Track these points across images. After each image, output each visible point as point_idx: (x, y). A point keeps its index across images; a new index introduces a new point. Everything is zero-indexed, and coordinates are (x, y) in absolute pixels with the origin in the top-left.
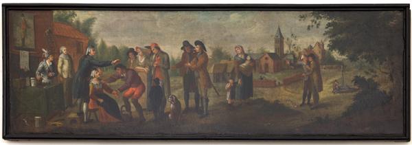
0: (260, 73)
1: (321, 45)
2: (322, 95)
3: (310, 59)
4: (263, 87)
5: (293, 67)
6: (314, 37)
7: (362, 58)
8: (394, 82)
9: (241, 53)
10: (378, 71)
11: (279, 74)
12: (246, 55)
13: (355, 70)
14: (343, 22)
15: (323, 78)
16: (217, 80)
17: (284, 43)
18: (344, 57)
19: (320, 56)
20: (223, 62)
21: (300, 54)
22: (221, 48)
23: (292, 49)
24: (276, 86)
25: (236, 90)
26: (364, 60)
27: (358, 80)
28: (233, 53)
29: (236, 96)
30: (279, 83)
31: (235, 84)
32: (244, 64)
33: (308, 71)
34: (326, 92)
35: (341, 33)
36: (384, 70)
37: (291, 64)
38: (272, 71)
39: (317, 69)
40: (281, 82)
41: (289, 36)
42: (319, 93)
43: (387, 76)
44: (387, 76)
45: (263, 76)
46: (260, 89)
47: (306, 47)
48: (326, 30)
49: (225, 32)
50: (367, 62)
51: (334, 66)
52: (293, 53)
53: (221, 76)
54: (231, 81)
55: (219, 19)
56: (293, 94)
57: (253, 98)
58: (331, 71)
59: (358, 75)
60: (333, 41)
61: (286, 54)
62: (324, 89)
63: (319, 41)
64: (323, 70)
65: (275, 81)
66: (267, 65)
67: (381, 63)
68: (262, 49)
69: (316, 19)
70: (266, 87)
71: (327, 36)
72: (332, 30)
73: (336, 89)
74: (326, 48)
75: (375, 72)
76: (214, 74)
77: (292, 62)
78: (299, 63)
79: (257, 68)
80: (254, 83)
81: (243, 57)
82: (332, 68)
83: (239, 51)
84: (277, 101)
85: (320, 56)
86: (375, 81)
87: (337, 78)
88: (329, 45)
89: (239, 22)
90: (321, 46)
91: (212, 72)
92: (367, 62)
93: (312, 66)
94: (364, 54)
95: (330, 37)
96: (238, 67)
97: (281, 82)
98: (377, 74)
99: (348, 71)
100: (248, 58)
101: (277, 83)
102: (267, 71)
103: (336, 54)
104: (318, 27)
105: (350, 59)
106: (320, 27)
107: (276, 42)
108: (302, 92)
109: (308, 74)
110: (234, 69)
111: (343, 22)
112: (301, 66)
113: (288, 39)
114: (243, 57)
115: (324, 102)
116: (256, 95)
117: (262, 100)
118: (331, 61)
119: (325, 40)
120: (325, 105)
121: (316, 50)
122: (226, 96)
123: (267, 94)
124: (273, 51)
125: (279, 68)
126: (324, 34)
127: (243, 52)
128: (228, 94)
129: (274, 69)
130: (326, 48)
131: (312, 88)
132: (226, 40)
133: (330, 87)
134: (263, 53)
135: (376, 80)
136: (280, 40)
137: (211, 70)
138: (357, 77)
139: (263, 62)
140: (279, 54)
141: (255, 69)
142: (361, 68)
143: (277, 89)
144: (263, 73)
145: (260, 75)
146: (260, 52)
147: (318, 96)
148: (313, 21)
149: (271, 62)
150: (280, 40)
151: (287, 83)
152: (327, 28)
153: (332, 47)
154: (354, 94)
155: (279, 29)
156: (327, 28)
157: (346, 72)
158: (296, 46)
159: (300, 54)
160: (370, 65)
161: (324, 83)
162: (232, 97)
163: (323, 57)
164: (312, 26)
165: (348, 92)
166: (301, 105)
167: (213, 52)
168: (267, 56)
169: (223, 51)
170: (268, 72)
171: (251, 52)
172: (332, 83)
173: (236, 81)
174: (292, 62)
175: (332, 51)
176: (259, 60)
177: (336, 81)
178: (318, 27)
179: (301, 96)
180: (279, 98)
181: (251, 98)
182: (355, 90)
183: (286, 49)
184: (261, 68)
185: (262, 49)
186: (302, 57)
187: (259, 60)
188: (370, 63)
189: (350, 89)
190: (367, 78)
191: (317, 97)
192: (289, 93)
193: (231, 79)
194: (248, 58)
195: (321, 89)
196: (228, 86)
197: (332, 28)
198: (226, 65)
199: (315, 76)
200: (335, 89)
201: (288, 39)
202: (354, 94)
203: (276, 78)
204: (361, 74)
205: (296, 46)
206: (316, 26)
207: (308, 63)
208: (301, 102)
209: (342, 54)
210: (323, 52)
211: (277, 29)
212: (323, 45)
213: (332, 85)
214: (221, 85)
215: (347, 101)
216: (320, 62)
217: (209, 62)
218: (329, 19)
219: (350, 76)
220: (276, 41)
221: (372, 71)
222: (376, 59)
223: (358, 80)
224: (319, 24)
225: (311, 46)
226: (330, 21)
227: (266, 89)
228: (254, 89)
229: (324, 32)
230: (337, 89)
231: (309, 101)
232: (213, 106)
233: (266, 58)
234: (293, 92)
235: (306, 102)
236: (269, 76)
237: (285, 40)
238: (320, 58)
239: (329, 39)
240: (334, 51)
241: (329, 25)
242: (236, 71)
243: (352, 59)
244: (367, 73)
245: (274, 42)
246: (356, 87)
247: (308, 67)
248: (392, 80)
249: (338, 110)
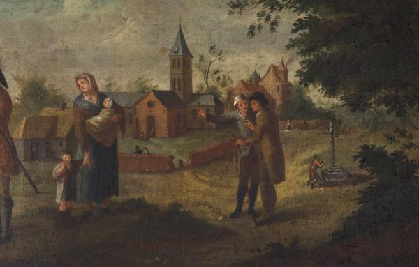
0: (137, 136)
1: (279, 72)
2: (283, 191)
3: (255, 106)
4: (142, 172)
6: (263, 53)
7: (378, 103)
9: (90, 92)
11: (181, 141)
12: (102, 97)
13: (360, 132)
14: (332, 17)
15: (287, 150)
16: (33, 156)
18: (336, 101)
19: (278, 98)
20: (47, 112)
21: (231, 94)
22: (44, 80)
24: (172, 169)
25: (79, 176)
26: (383, 108)
27: (368, 156)
28: (70, 92)
29: (78, 195)
30: (181, 161)
31: (75, 164)
32: (99, 118)
33: (251, 133)
34: (293, 184)
35: (328, 43)
37: (209, 117)
38: (165, 134)
39: (271, 130)
40: (186, 161)
41: (205, 51)
45: (142, 145)
46: (136, 176)
47: (245, 76)
48: (294, 36)
49: (52, 40)
50: (389, 112)
51: (312, 122)
52: (213, 92)
53: (42, 147)
54: (65, 157)
55: (37, 11)
57: (120, 198)
58: (305, 133)
60: (309, 63)
61: (199, 95)
62: (288, 175)
64: (284, 132)
65: (172, 157)
66: (151, 121)
69: (268, 10)
70: (150, 172)
71: (296, 49)
73: (316, 175)
74: (292, 78)
75: (411, 136)
76: (26, 141)
77: (212, 112)
78: (228, 114)
79: (127, 126)
81: (94, 101)
82: (306, 127)
83: (86, 86)
84: (176, 205)
85: (278, 98)
86: (410, 158)
87: (317, 151)
88: (299, 73)
89: (85, 17)
90: (281, 76)
91: (20, 135)
92: (389, 112)
93: (260, 122)
94: (383, 93)
95: (303, 53)
96: (83, 124)
98: (414, 141)
99: (345, 133)
100: (108, 103)
101: (176, 162)
102: (151, 134)
103: (316, 95)
104: (273, 29)
106: (280, 29)
108: (236, 183)
109: (250, 140)
110: (72, 132)
111: (332, 17)
112: (233, 122)
113: (202, 58)
114: (94, 101)
115: (289, 207)
116: (126, 192)
117: (140, 204)
118: (305, 110)
119: (291, 61)
120: (291, 216)
121: (270, 85)
122: (54, 193)
123: (150, 189)
124: (165, 86)
125: (179, 127)
126: (288, 47)
127: (94, 88)
128: (60, 190)
129: (169, 128)
130: (292, 78)
131: (259, 173)
132: (54, 60)
133: (303, 173)
134: (144, 91)
135: (411, 155)
136: (182, 61)
137: (18, 132)
138: (366, 147)
139: (143, 112)
140: (180, 94)
141: (123, 132)
142: (376, 126)
146: (135, 88)
148: (260, 15)
149: (161, 113)
150: (182, 61)
151: (200, 162)
152: (294, 31)
153: (308, 77)
154: (360, 187)
155: (181, 32)
156: (294, 31)
157: (341, 136)
158: (221, 75)
159: (231, 94)
160: (398, 120)
161: (287, 162)
162: (69, 195)
163: (286, 103)
164: (260, 27)
165: (346, 183)
166: (234, 215)
167: (23, 91)
168: (152, 97)
170: (154, 136)
171: (113, 89)
172: (306, 162)
173: (78, 158)
174: (212, 112)
175: (306, 85)
176: (134, 108)
177: (316, 157)
178: (273, 29)
179: (232, 193)
180: (182, 198)
181: (114, 198)
182: (361, 179)
183: (197, 81)
186: (237, 100)
188: (399, 115)
189: (351, 176)
190: (390, 149)
191: (270, 195)
192: (204, 187)
193: (67, 152)
194: (108, 103)
195: (281, 177)
196: (59, 169)
197: (307, 31)
198: (55, 120)
199: (266, 147)
200: (313, 174)
201: (202, 58)
202: (360, 187)
204: (377, 142)
205: (221, 75)
206: (267, 26)
207: (251, 115)
208: (233, 208)
209: (331, 92)
210: (286, 88)
212: (286, 73)
213: (306, 167)
214: (41, 167)
215: (343, 205)
216: (278, 113)
217: (14, 112)
218: (303, 9)
219: (350, 146)
220: (174, 64)
221: (403, 134)
222: (411, 105)
223: (368, 156)
224: (275, 23)
225: (256, 78)
226: (303, 16)
227: (150, 176)
228: (121, 176)
229: (288, 42)
230: (319, 177)
231: (252, 203)
232: (22, 217)
233: (151, 104)
234: (212, 184)
235: (246, 207)
236: (159, 147)
237: (195, 61)
238: (278, 103)
239: (300, 59)
240: (311, 87)
241: (300, 25)
242: (78, 134)
243: (356, 104)
244: (390, 139)
245: (168, 64)
246: (365, 172)
247: (249, 124)
249: (322, 227)
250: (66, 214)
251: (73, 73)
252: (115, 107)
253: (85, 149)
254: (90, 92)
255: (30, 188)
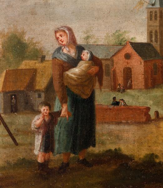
0: (114, 88)
4: (119, 123)
12: (80, 49)
20: (25, 65)
22: (23, 33)
24: (148, 120)
29: (57, 146)
30: (157, 113)
31: (54, 116)
32: (76, 70)
45: (119, 96)
46: (113, 127)
54: (44, 109)
57: (96, 150)
65: (148, 109)
66: (128, 73)
68: (118, 35)
79: (105, 77)
80: (98, 116)
81: (73, 53)
83: (65, 39)
96: (62, 76)
100: (86, 55)
101: (152, 113)
102: (128, 85)
110: (50, 86)
114: (73, 53)
116: (103, 143)
122: (32, 144)
124: (142, 38)
127: (73, 40)
128: (38, 141)
132: (33, 13)
134: (121, 44)
139: (120, 65)
145: (113, 95)
146: (112, 41)
149: (138, 65)
162: (48, 146)
168: (129, 49)
169: (26, 38)
170: (130, 87)
171: (91, 41)
173: (56, 109)
176: (111, 60)
181: (91, 149)
187: (111, 60)
193: (46, 104)
194: (86, 55)
196: (37, 120)
198: (34, 72)
203: (150, 103)
214: (20, 119)
227: (126, 127)
228: (99, 128)
233: (128, 56)
236: (136, 98)
242: (56, 86)
250: (44, 166)
251: (52, 26)
252: (94, 60)
253: (63, 101)
254: (68, 45)
255: (9, 139)
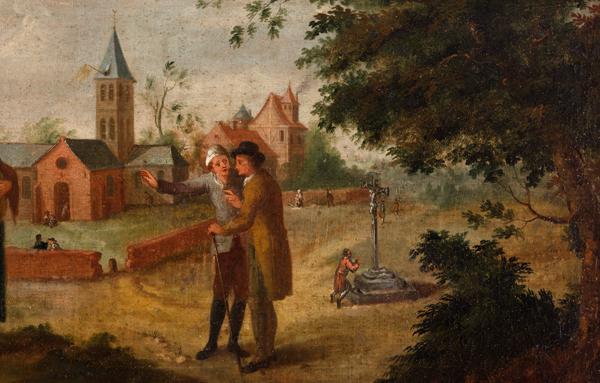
1: (285, 106)
2: (289, 313)
3: (243, 165)
4: (47, 280)
5: (169, 199)
8: (589, 255)
10: (519, 210)
11: (114, 227)
14: (376, 11)
15: (295, 243)
17: (137, 100)
18: (381, 155)
19: (281, 151)
21: (200, 145)
23: (168, 125)
24: (98, 275)
26: (463, 167)
27: (437, 250)
30: (113, 262)
33: (235, 213)
35: (367, 55)
36: (543, 208)
37: (162, 186)
38: (86, 213)
39: (270, 207)
40: (122, 261)
41: (157, 71)
42: (275, 303)
43: (559, 230)
44: (559, 230)
45: (47, 234)
46: (36, 287)
47: (226, 116)
48: (311, 44)
50: (473, 174)
51: (340, 192)
56: (170, 310)
58: (327, 211)
59: (439, 229)
60: (336, 91)
61: (145, 147)
63: (281, 91)
64: (291, 211)
65: (98, 255)
66: (62, 192)
67: (533, 181)
68: (45, 126)
70: (61, 280)
71: (314, 67)
72: (336, 43)
73: (346, 284)
74: (307, 118)
75: (510, 216)
77: (169, 177)
78: (195, 179)
79: (22, 200)
82: (329, 200)
84: (104, 338)
85: (281, 151)
86: (509, 253)
87: (349, 242)
88: (319, 108)
90: (288, 113)
92: (473, 174)
94: (463, 140)
95: (325, 73)
97: (122, 261)
98: (517, 224)
101: (104, 263)
102: (62, 214)
103: (348, 146)
104: (273, 32)
105: (405, 161)
106: (285, 32)
107: (102, 96)
108: (208, 299)
109: (232, 224)
112: (202, 194)
113: (151, 83)
115: (300, 339)
116: (19, 315)
117: (42, 337)
118: (327, 172)
119: (304, 86)
121: (269, 132)
124: (87, 132)
125: (111, 203)
126: (300, 63)
129: (94, 205)
130: (307, 118)
131: (246, 280)
133: (323, 280)
135: (511, 248)
136: (118, 90)
139: (48, 177)
140: (113, 145)
141: (15, 211)
142: (451, 197)
143: (104, 287)
144: (47, 223)
145: (37, 230)
146: (35, 136)
147: (273, 315)
149: (80, 178)
150: (118, 90)
151: (145, 262)
152: (311, 36)
153: (333, 116)
154: (422, 304)
155: (115, 36)
156: (311, 36)
158: (184, 112)
159: (200, 145)
163: (296, 159)
164: (251, 30)
166: (202, 356)
168: (65, 151)
170: (67, 218)
172: (329, 262)
174: (169, 177)
175: (331, 129)
176: (33, 169)
177: (346, 252)
178: (273, 32)
179: (204, 315)
180: (113, 326)
182: (422, 291)
183: (142, 124)
184: (39, 202)
185: (45, 126)
186: (211, 156)
187: (33, 169)
188: (490, 178)
189: (405, 284)
191: (266, 321)
192: (153, 306)
195: (284, 287)
197: (333, 35)
199: (260, 237)
200: (342, 285)
201: (151, 83)
202: (422, 304)
203: (101, 246)
204: (451, 226)
205: (184, 112)
207: (234, 181)
208: (202, 342)
209: (374, 139)
210: (296, 135)
211: (110, 35)
212: (295, 108)
213: (329, 270)
216: (281, 177)
219: (404, 234)
220: (103, 94)
221: (496, 211)
222: (511, 161)
223: (437, 250)
224: (276, 22)
227: (60, 287)
229: (299, 54)
230: (350, 287)
233: (62, 163)
234: (168, 301)
235: (224, 340)
236: (76, 236)
237: (139, 88)
238: (283, 160)
239: (321, 83)
240: (338, 131)
243: (416, 162)
244: (474, 220)
246: (430, 279)
247: (231, 197)
248: (579, 248)
